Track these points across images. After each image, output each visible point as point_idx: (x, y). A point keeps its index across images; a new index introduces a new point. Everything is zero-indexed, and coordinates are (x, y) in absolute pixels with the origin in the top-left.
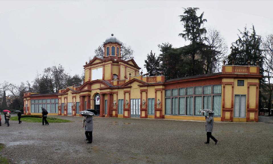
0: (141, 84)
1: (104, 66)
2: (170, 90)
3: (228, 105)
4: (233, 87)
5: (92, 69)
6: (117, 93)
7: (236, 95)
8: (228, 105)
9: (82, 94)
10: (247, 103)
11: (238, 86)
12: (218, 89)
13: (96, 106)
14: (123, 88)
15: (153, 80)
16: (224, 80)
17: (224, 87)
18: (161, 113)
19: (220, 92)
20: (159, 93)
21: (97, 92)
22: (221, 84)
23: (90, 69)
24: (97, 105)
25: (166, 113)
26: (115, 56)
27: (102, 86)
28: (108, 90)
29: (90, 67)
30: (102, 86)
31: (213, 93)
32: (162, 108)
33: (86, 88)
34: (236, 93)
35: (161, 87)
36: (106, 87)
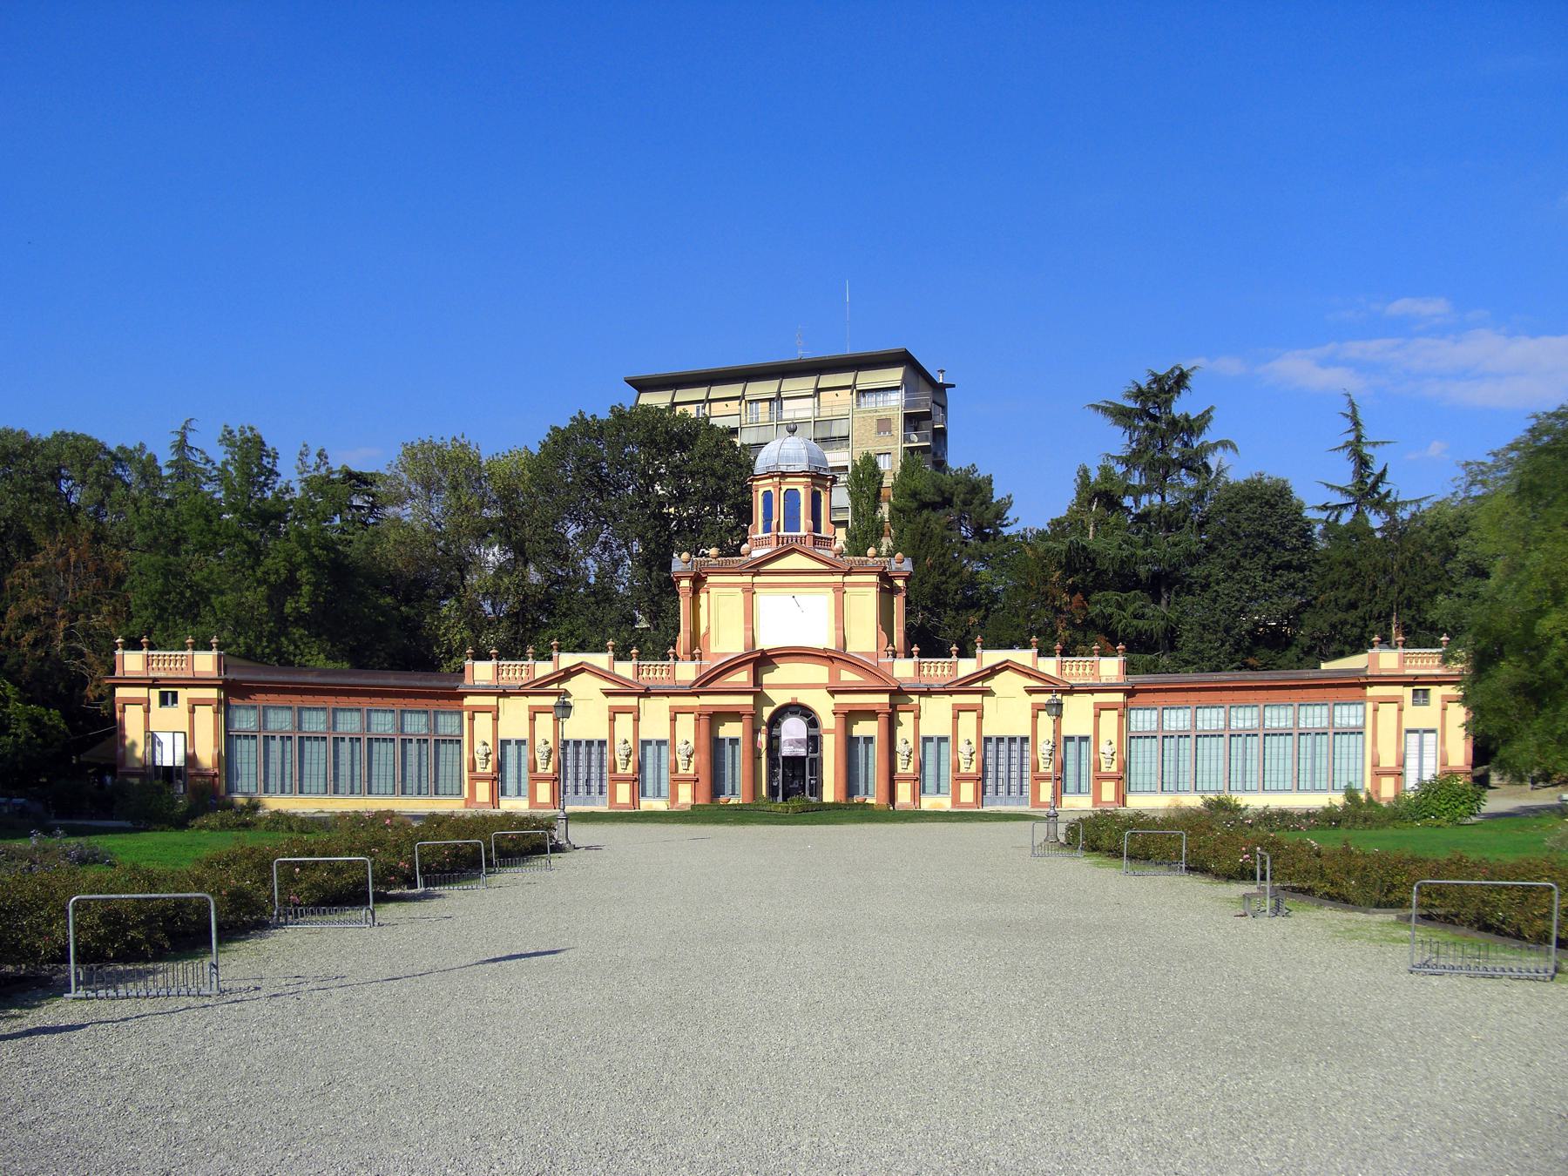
3: (1388, 761)
4: (1401, 710)
7: (1409, 731)
8: (1388, 761)
10: (1441, 751)
11: (1413, 705)
12: (1347, 715)
14: (951, 693)
16: (1370, 691)
17: (1376, 710)
19: (1360, 722)
20: (1110, 719)
22: (1361, 701)
27: (848, 676)
28: (885, 698)
30: (848, 676)
33: (742, 677)
34: (1406, 725)
35: (1119, 697)
36: (874, 683)
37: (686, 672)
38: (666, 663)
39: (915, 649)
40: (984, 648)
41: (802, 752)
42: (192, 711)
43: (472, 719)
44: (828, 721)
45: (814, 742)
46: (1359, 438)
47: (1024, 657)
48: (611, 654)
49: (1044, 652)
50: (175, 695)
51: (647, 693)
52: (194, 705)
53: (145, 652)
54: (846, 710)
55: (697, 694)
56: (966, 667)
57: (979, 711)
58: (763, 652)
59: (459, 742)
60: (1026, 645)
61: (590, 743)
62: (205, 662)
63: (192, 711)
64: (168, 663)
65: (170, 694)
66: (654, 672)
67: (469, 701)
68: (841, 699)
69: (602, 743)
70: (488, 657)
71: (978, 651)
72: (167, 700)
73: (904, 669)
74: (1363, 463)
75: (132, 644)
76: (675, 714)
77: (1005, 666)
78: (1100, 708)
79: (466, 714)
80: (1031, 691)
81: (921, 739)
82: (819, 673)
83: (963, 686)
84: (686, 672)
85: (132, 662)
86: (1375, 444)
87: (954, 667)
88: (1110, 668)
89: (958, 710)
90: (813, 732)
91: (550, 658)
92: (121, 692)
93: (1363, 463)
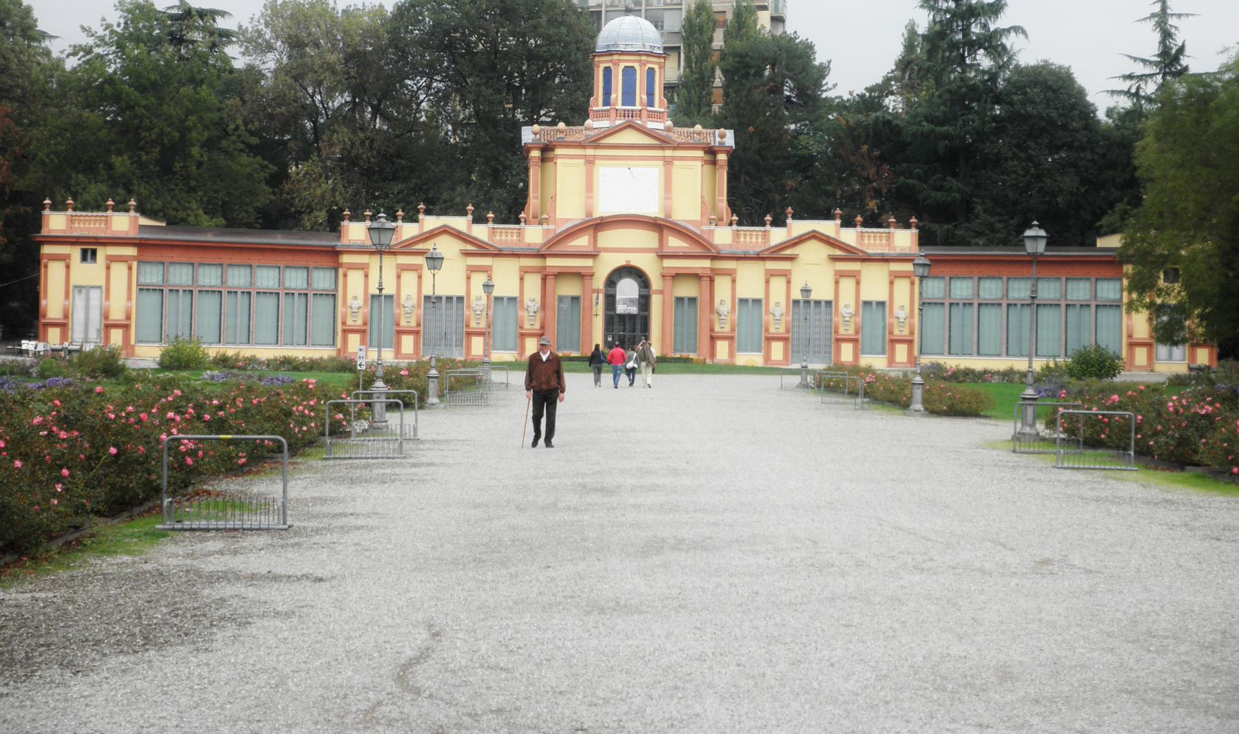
0: (838, 253)
1: (668, 162)
2: (1001, 278)
5: (597, 161)
6: (731, 274)
9: (550, 262)
13: (616, 320)
14: (764, 259)
15: (878, 241)
18: (910, 351)
20: (902, 287)
21: (633, 263)
23: (590, 162)
24: (622, 317)
25: (921, 352)
26: (638, 107)
28: (706, 264)
29: (590, 152)
30: (674, 243)
31: (1096, 297)
32: (912, 333)
33: (582, 242)
36: (697, 250)
37: (533, 235)
38: (517, 226)
39: (735, 218)
40: (794, 217)
41: (634, 310)
42: (108, 268)
43: (345, 275)
44: (656, 283)
45: (644, 302)
46: (1164, 9)
47: (827, 227)
48: (470, 217)
49: (847, 223)
50: (94, 252)
51: (499, 254)
52: (112, 259)
53: (70, 212)
54: (673, 272)
55: (543, 256)
56: (778, 235)
57: (786, 274)
58: (602, 218)
59: (334, 296)
60: (828, 216)
61: (449, 299)
62: (122, 223)
63: (108, 268)
64: (89, 224)
65: (89, 252)
66: (505, 235)
67: (346, 259)
68: (668, 263)
69: (460, 299)
70: (363, 219)
71: (789, 221)
72: (88, 255)
73: (723, 236)
74: (1166, 35)
75: (58, 207)
76: (524, 271)
77: (814, 236)
78: (895, 276)
79: (341, 271)
80: (835, 259)
81: (737, 301)
82: (647, 238)
83: (775, 254)
84: (533, 235)
85: (56, 222)
86: (1179, 16)
87: (766, 235)
88: (904, 239)
89: (770, 274)
90: (644, 292)
91: (416, 221)
92: (47, 250)
93: (1166, 35)
